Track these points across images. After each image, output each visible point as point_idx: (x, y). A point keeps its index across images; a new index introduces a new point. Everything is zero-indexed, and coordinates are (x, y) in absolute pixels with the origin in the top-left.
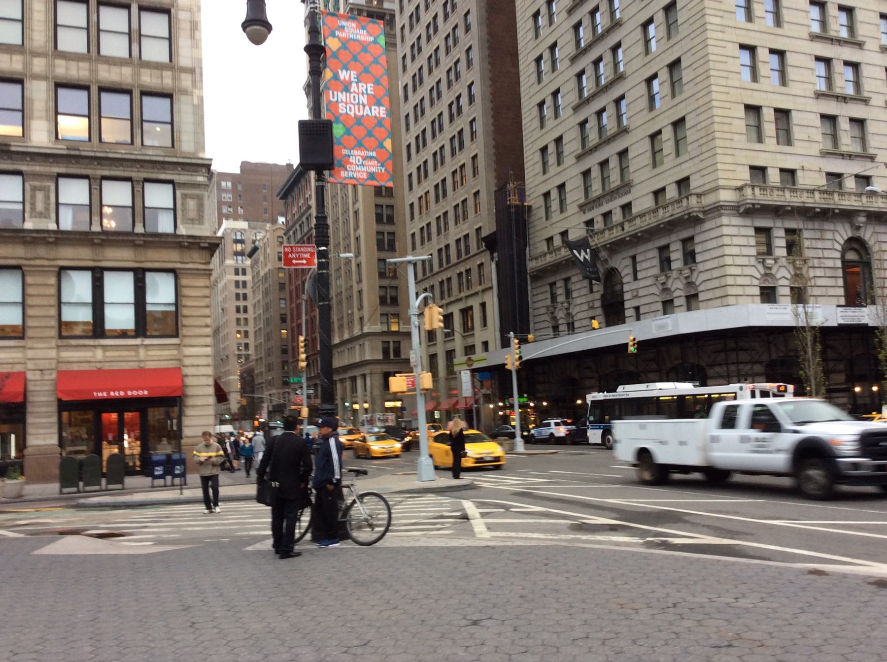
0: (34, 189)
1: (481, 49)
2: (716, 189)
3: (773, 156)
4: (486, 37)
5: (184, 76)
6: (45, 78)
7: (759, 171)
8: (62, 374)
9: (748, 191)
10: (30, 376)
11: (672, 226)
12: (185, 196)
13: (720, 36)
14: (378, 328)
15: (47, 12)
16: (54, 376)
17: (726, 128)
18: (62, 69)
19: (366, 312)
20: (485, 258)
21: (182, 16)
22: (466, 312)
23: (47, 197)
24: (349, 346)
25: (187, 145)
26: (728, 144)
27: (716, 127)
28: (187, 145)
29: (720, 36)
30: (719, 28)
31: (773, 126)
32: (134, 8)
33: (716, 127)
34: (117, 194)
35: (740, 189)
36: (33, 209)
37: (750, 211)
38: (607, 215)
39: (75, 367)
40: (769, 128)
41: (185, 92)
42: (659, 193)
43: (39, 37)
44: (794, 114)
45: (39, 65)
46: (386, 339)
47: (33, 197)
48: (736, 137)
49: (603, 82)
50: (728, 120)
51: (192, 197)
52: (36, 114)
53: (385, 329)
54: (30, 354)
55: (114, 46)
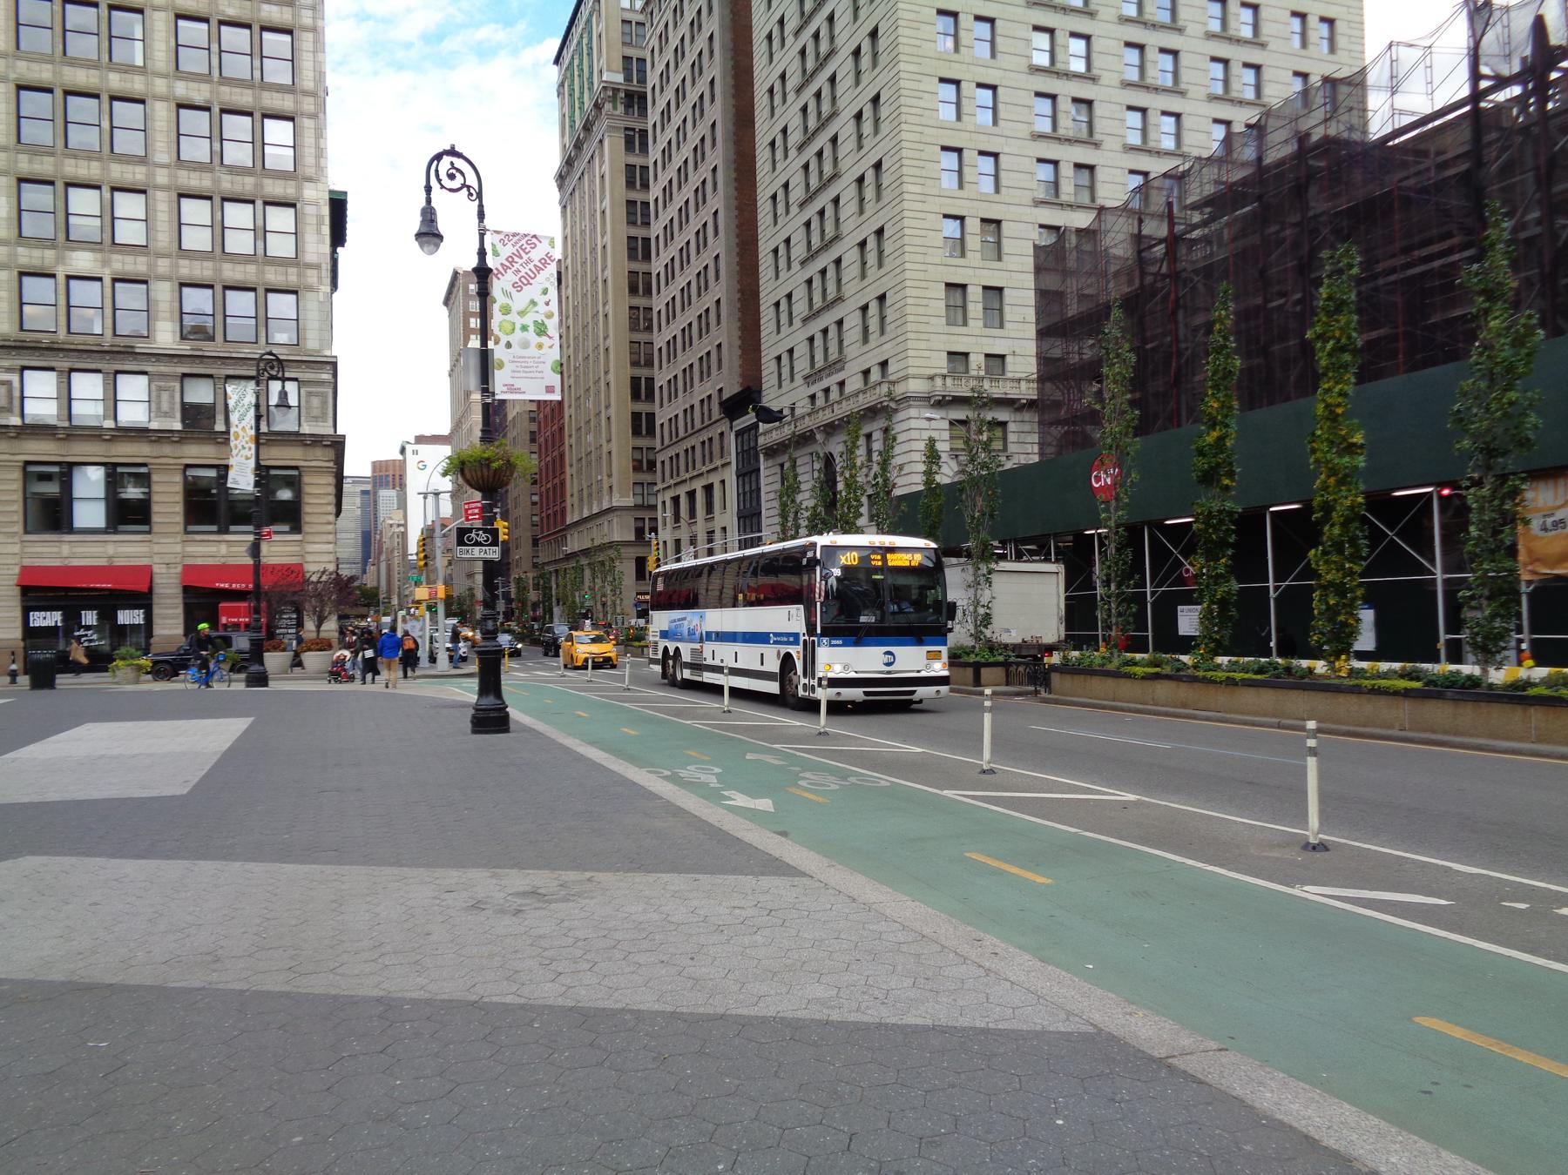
0: (160, 389)
1: (726, 169)
2: (906, 378)
3: (977, 340)
4: (732, 156)
5: (310, 272)
6: (168, 279)
7: (959, 357)
8: (187, 568)
9: (939, 381)
10: (156, 569)
11: (873, 412)
12: (310, 394)
13: (919, 206)
14: (629, 501)
15: (170, 212)
16: (179, 569)
17: (921, 310)
18: (187, 269)
19: (614, 481)
20: (723, 426)
21: (309, 210)
22: (709, 489)
23: (172, 397)
24: (598, 521)
25: (312, 343)
26: (922, 328)
27: (909, 309)
28: (312, 343)
29: (919, 206)
31: (980, 306)
32: (259, 203)
33: (909, 309)
35: (931, 378)
36: (159, 409)
37: (942, 403)
38: (827, 391)
39: (199, 562)
40: (975, 308)
41: (310, 289)
42: (866, 373)
43: (164, 239)
44: (1006, 292)
45: (163, 265)
46: (640, 514)
47: (159, 397)
48: (933, 320)
49: (827, 238)
50: (924, 302)
51: (316, 395)
52: (161, 315)
53: (640, 501)
54: (156, 548)
55: (239, 243)
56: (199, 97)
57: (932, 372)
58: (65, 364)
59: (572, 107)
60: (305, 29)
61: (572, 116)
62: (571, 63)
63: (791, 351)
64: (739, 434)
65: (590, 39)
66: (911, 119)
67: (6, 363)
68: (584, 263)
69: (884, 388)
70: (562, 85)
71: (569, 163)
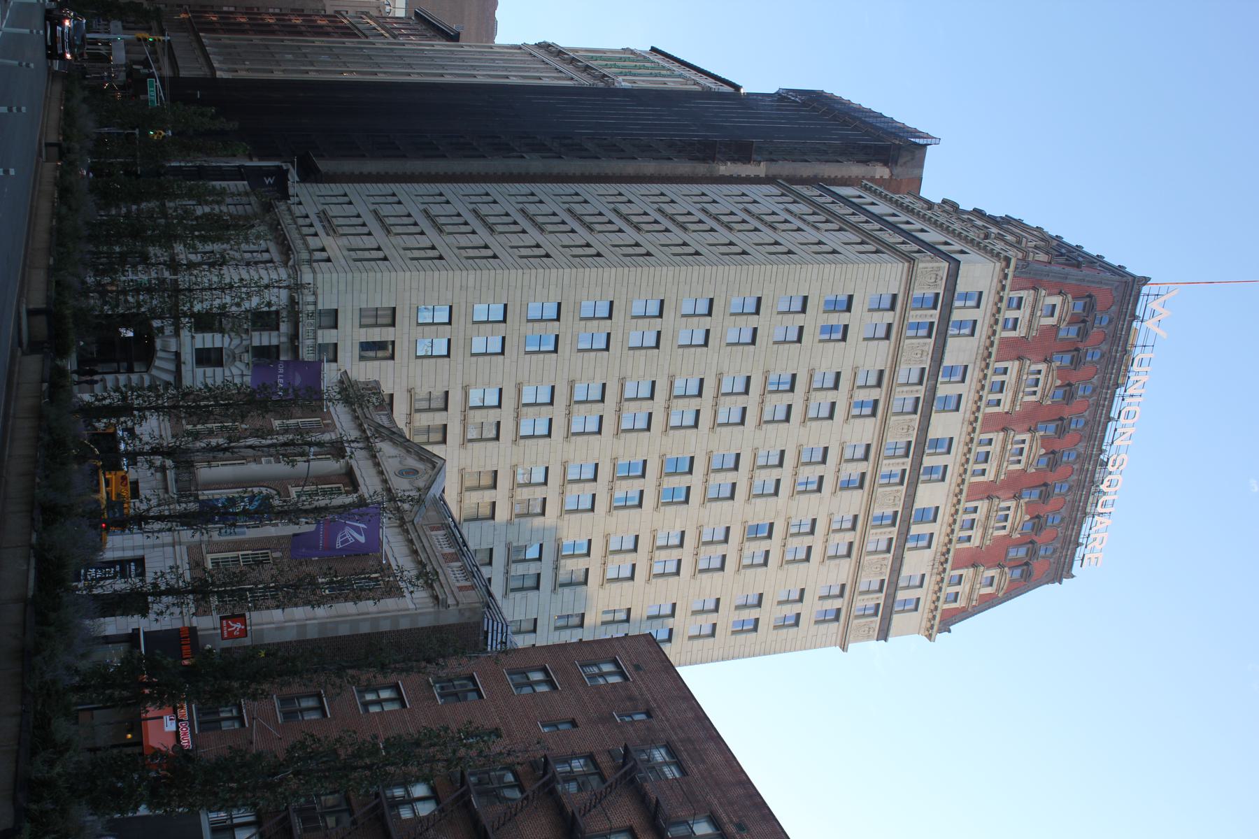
2: (314, 272)
7: (332, 318)
9: (311, 299)
13: (457, 285)
30: (464, 284)
38: (311, 225)
40: (376, 335)
57: (319, 291)
59: (609, 59)
61: (601, 58)
62: (649, 61)
65: (664, 76)
66: (526, 277)
68: (463, 60)
69: (305, 255)
70: (632, 52)
71: (559, 53)
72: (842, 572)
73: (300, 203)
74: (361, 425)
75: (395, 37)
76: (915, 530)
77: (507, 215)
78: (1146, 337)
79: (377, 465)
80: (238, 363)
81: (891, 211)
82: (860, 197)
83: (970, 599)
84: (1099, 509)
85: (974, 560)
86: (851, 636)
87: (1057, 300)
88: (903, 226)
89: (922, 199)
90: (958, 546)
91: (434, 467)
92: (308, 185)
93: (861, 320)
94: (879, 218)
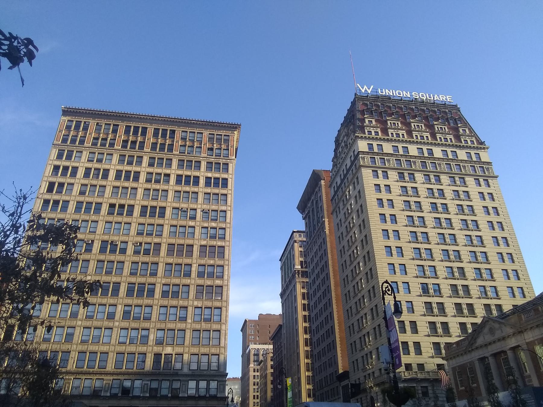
0: (183, 384)
12: (220, 384)
25: (222, 370)
34: (203, 384)
40: (412, 349)
41: (222, 354)
56: (200, 305)
58: (160, 378)
59: (285, 274)
60: (225, 285)
61: (285, 277)
62: (285, 262)
63: (357, 360)
64: (343, 387)
67: (148, 379)
72: (470, 180)
73: (359, 379)
74: (469, 351)
75: (282, 347)
76: (450, 157)
77: (356, 303)
78: (374, 92)
79: (490, 344)
80: (430, 403)
81: (339, 177)
82: (334, 187)
83: (472, 136)
84: (432, 99)
85: (458, 137)
86: (492, 175)
87: (367, 120)
88: (345, 172)
89: (332, 169)
90: (454, 142)
91: (488, 321)
92: (350, 376)
93: (382, 181)
94: (342, 181)
